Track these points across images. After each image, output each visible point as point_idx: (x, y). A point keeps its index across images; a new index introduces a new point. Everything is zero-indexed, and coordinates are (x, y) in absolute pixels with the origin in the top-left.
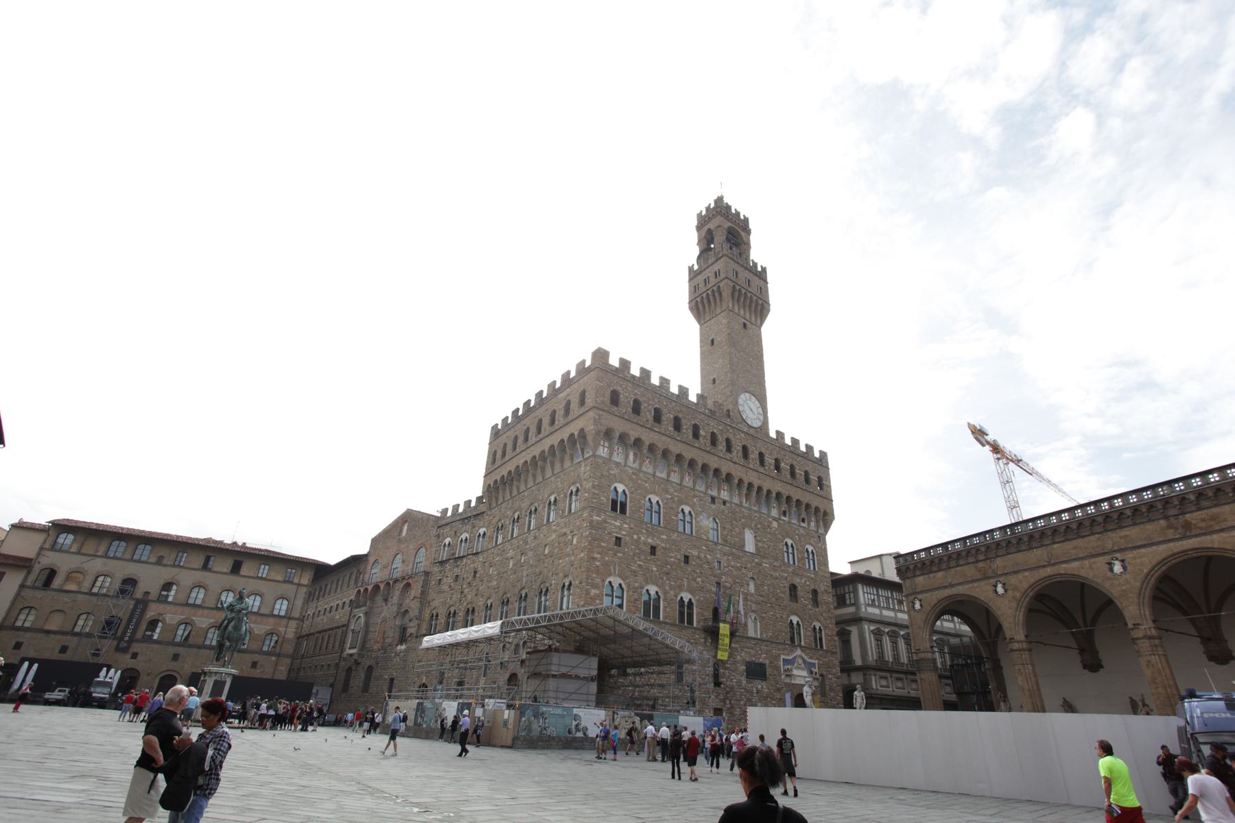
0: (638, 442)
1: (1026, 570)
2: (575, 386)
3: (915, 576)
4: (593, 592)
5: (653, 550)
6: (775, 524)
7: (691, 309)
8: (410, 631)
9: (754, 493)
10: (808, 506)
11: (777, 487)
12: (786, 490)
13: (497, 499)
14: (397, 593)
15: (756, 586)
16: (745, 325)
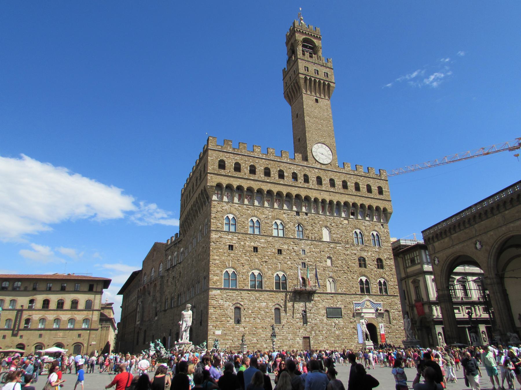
0: (240, 188)
1: (491, 231)
2: (202, 161)
3: (434, 242)
4: (215, 278)
5: (256, 249)
6: (346, 222)
7: (285, 97)
8: (158, 309)
9: (327, 206)
10: (370, 207)
11: (343, 199)
12: (351, 200)
13: (185, 231)
14: (152, 289)
15: (331, 261)
16: (317, 101)
